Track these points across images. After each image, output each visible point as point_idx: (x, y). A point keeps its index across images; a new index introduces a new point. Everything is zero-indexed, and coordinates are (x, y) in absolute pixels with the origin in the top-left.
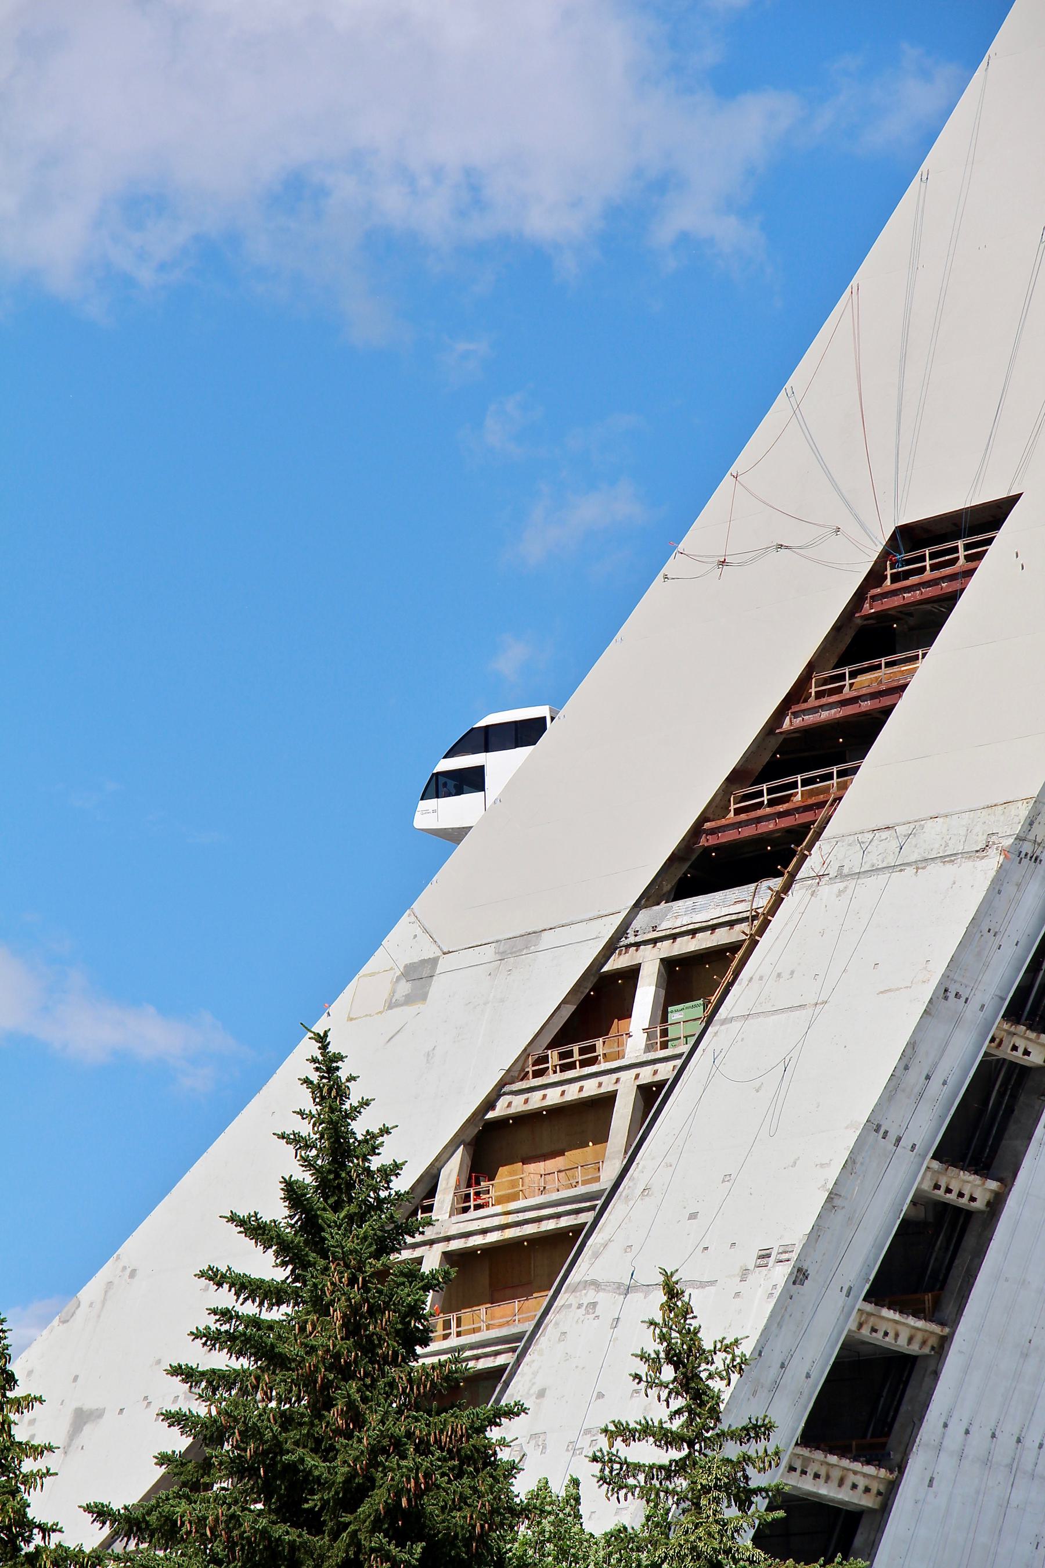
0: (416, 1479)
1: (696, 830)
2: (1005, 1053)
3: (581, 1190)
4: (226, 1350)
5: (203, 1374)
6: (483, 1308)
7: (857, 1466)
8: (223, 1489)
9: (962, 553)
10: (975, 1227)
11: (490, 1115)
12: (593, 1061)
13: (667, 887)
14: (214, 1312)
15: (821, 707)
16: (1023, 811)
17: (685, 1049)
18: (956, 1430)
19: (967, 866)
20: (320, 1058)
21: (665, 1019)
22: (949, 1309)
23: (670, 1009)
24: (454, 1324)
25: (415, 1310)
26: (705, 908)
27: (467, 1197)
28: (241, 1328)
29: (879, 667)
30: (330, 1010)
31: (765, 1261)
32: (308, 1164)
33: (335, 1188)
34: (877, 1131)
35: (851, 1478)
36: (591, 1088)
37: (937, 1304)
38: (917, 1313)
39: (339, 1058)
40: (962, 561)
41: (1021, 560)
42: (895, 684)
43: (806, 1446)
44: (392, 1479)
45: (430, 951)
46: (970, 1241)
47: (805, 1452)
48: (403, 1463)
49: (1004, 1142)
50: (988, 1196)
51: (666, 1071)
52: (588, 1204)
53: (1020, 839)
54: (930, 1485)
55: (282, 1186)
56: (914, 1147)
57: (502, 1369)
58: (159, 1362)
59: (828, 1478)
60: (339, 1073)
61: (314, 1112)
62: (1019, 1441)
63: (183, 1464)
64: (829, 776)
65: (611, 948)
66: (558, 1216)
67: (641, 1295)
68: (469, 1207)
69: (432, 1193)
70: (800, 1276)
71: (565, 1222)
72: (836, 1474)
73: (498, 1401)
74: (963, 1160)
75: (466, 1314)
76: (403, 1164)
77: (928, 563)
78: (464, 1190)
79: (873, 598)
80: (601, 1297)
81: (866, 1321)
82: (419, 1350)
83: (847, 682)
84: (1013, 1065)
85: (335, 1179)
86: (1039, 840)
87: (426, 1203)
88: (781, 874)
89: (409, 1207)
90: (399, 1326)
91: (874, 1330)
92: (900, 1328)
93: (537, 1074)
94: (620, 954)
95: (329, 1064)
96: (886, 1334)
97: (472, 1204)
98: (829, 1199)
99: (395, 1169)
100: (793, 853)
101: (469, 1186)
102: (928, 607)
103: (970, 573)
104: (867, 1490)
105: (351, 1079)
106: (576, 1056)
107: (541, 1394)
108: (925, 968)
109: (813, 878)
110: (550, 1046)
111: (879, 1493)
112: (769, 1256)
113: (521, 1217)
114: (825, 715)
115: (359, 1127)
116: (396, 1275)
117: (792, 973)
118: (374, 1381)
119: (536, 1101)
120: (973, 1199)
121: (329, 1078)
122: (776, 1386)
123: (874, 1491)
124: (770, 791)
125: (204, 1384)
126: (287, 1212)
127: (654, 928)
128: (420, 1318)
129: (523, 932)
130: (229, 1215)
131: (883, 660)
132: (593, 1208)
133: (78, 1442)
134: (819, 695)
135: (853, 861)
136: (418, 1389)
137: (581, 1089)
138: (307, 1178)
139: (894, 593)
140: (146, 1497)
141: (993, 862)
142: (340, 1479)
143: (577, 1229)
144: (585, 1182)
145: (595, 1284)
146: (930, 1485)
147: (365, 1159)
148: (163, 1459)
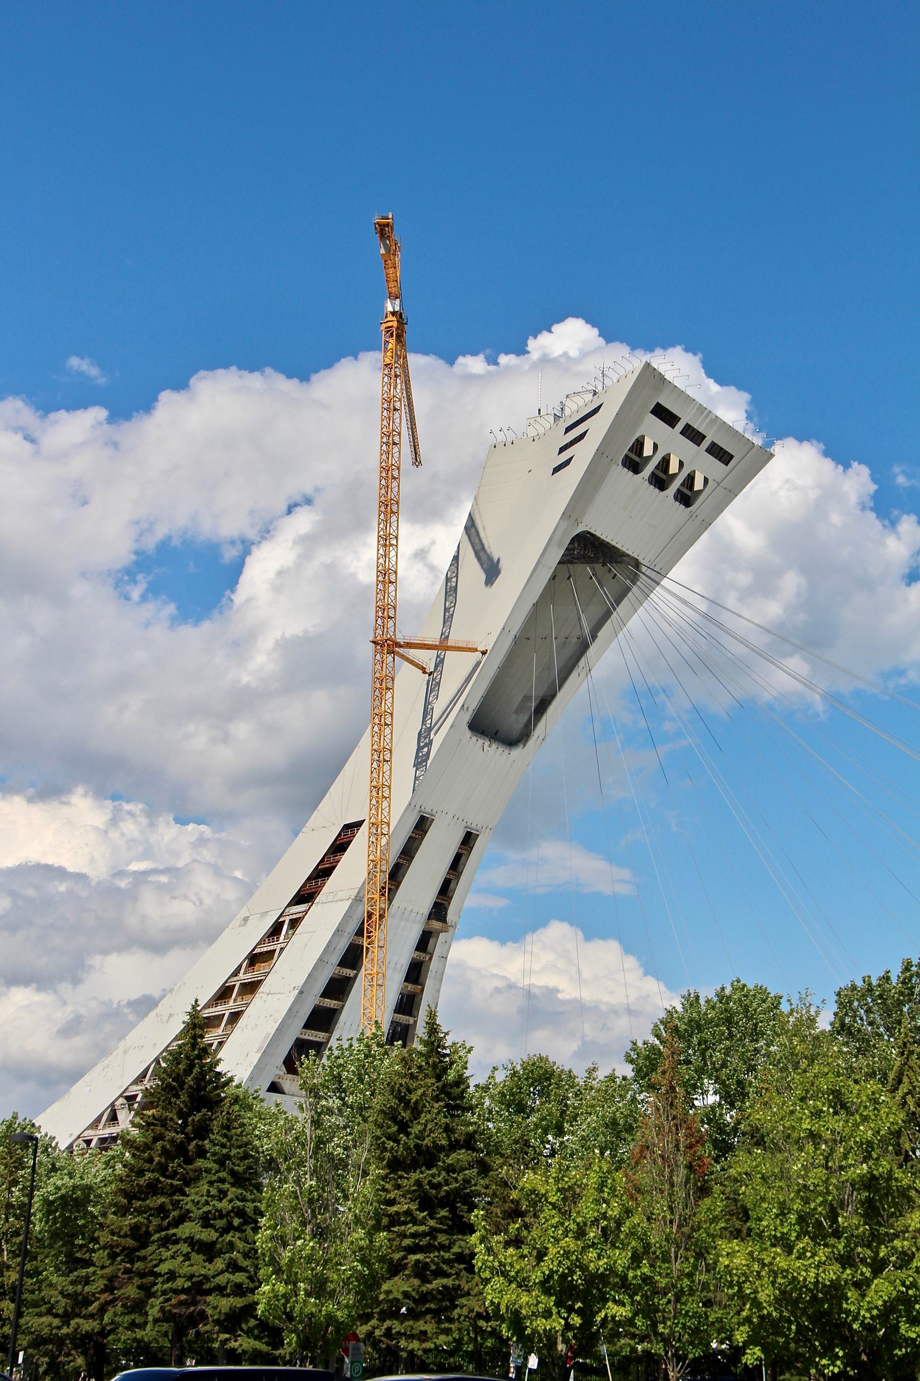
22: (345, 999)
37: (343, 997)
46: (350, 983)
65: (280, 916)
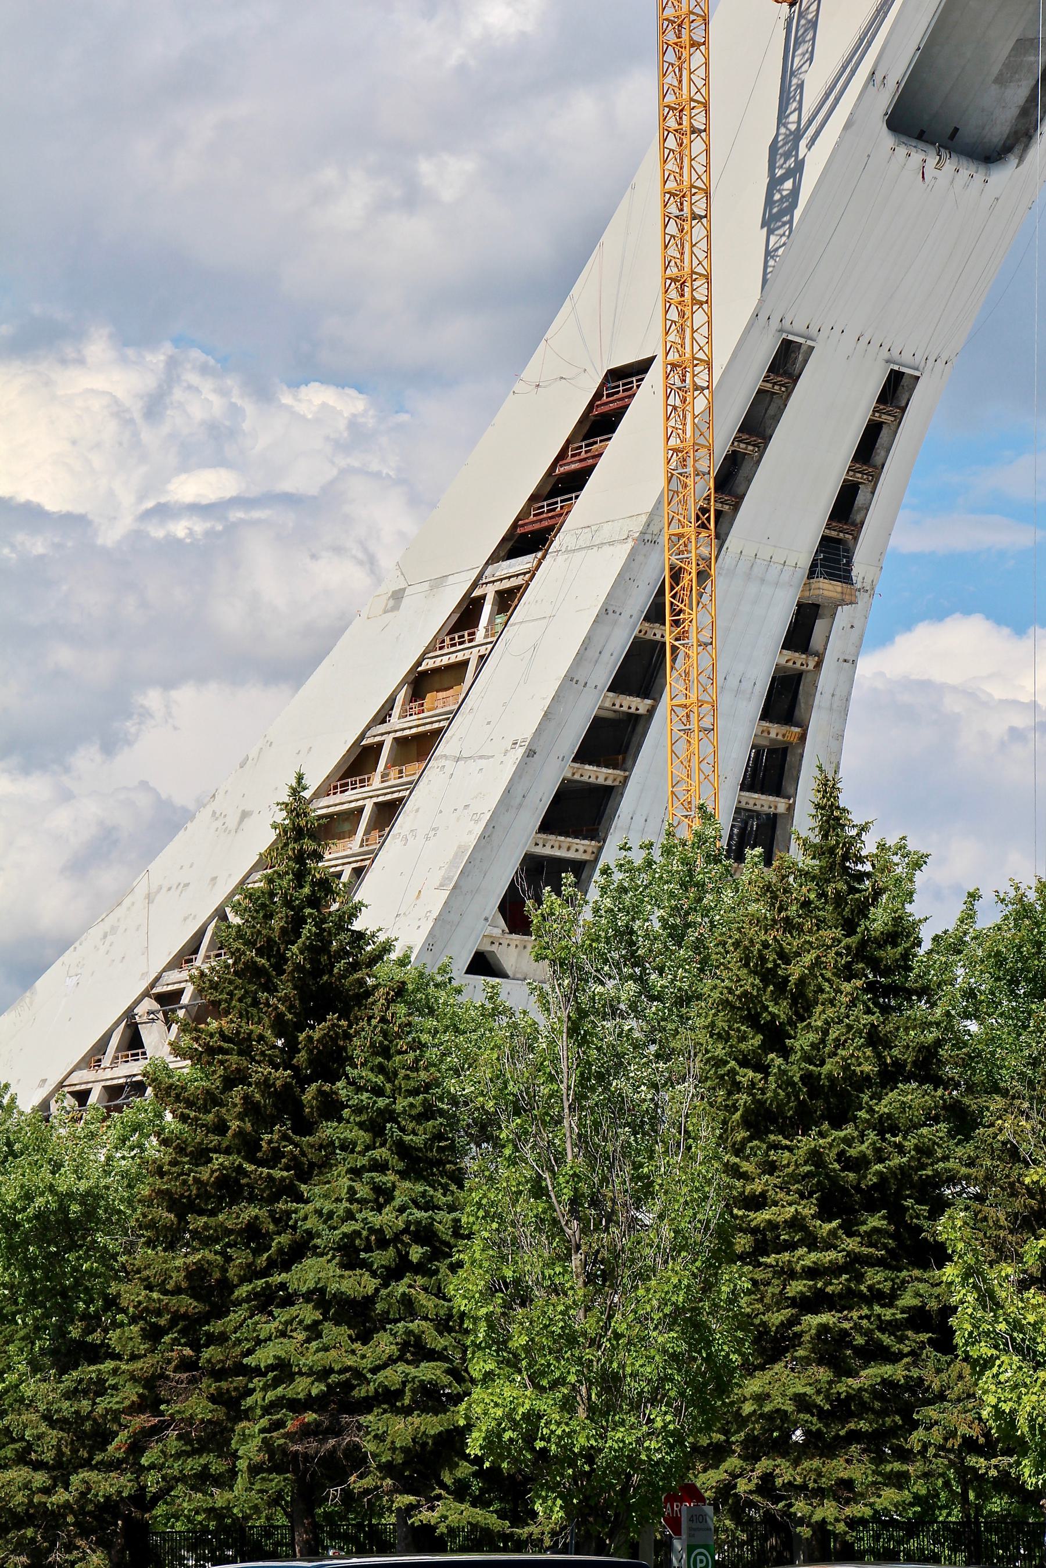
1: (515, 525)
11: (420, 669)
13: (502, 554)
16: (644, 519)
17: (495, 639)
26: (514, 566)
45: (403, 585)
65: (475, 585)
70: (531, 753)
79: (598, 406)
106: (457, 640)
114: (573, 466)
134: (573, 456)
141: (630, 544)
145: (445, 756)
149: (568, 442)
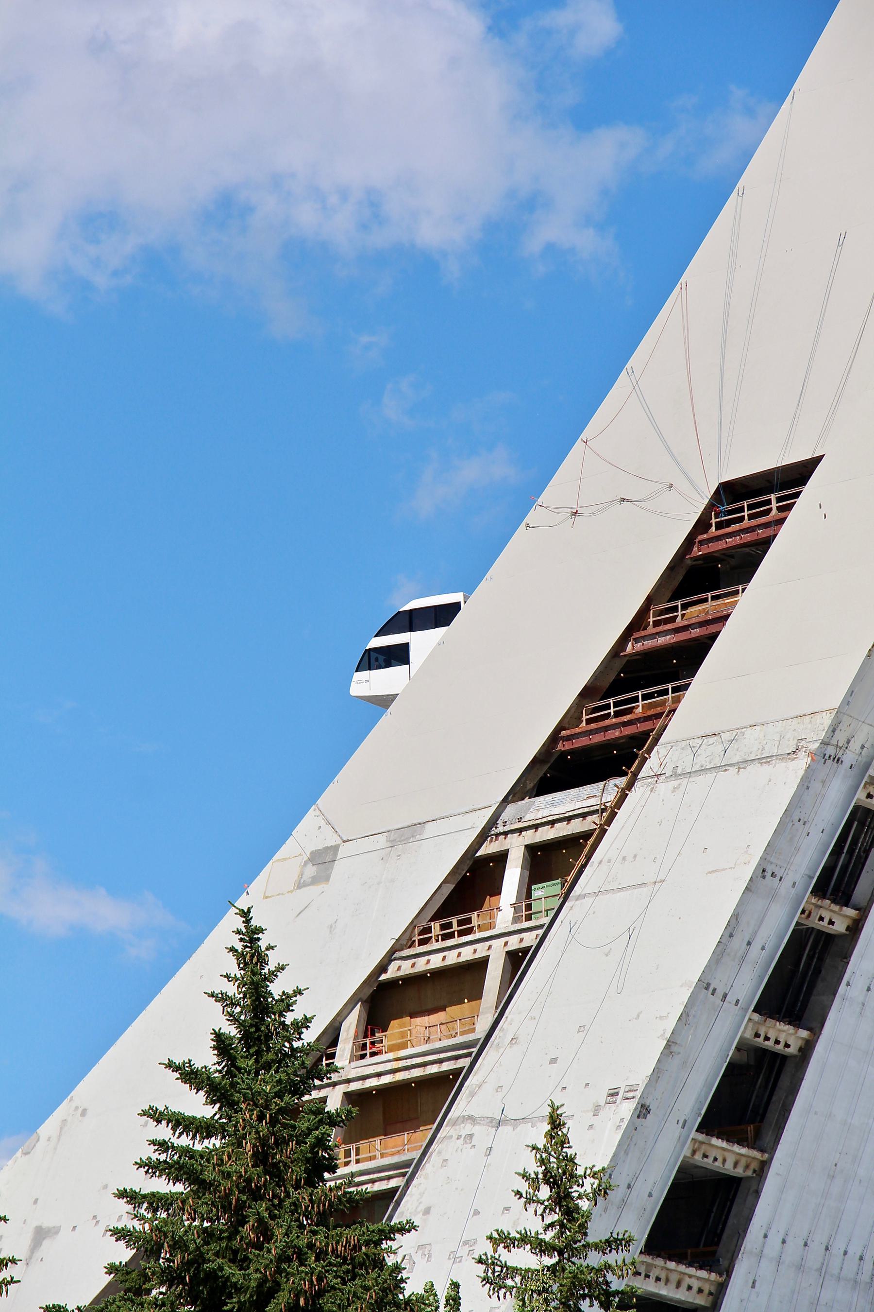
0: (311, 1282)
1: (554, 738)
2: (813, 923)
3: (460, 1039)
4: (164, 1177)
5: (144, 1197)
6: (377, 1140)
7: (692, 1271)
8: (161, 1293)
9: (774, 505)
10: (789, 1069)
11: (383, 977)
12: (470, 931)
13: (530, 785)
14: (153, 1143)
15: (658, 634)
16: (827, 720)
17: (546, 920)
18: (775, 1240)
19: (781, 766)
20: (244, 930)
21: (529, 895)
22: (768, 1138)
23: (533, 887)
24: (353, 1153)
25: (321, 1142)
26: (561, 802)
27: (364, 1047)
28: (176, 1158)
29: (706, 600)
30: (249, 890)
31: (614, 1098)
32: (233, 1019)
33: (256, 1039)
34: (707, 988)
35: (687, 1281)
36: (467, 954)
37: (758, 1134)
38: (741, 1141)
39: (260, 930)
40: (774, 511)
41: (824, 511)
42: (720, 614)
43: (649, 1254)
44: (293, 1283)
45: (332, 840)
46: (785, 1081)
47: (648, 1259)
48: (302, 1268)
49: (813, 998)
50: (800, 1043)
51: (530, 939)
52: (465, 1051)
53: (825, 743)
54: (753, 1286)
55: (213, 1037)
56: (737, 1002)
57: (394, 1190)
58: (106, 1187)
59: (667, 1281)
60: (260, 943)
61: (239, 976)
62: (827, 1249)
63: (128, 1273)
64: (665, 692)
65: (484, 836)
66: (440, 1061)
67: (510, 1128)
68: (366, 1054)
69: (334, 1043)
70: (643, 1111)
71: (446, 1067)
72: (674, 1277)
73: (390, 1218)
74: (779, 1013)
75: (363, 1145)
76: (312, 1018)
77: (746, 513)
78: (361, 1040)
79: (701, 543)
80: (477, 1130)
81: (699, 1149)
82: (326, 1175)
83: (680, 613)
84: (820, 933)
85: (255, 1032)
86: (840, 745)
87: (330, 1051)
88: (625, 774)
89: (316, 1054)
90: (309, 1155)
91: (705, 1156)
92: (727, 1154)
93: (423, 942)
94: (491, 841)
95: (251, 935)
96: (715, 1159)
97: (368, 1051)
98: (668, 1046)
99: (306, 1022)
100: (636, 756)
101: (365, 1036)
102: (747, 550)
103: (781, 522)
104: (700, 1291)
105: (270, 948)
106: (455, 927)
107: (427, 1211)
108: (746, 852)
109: (652, 777)
110: (433, 919)
111: (710, 1294)
112: (617, 1094)
113: (409, 1062)
114: (661, 641)
115: (276, 989)
116: (306, 1113)
117: (635, 856)
118: (281, 1201)
119: (421, 965)
120: (787, 1046)
121: (251, 947)
122: (624, 1203)
123: (706, 1292)
124: (616, 704)
125: (145, 1205)
126: (216, 1059)
127: (520, 820)
128: (327, 1148)
129: (409, 823)
130: (167, 1062)
131: (710, 595)
132: (469, 1055)
133: (38, 1254)
134: (656, 624)
135: (685, 763)
136: (318, 1207)
137: (459, 955)
138: (231, 1030)
139: (718, 538)
140: (96, 1300)
141: (802, 763)
142: (253, 1284)
143: (457, 1072)
144: (463, 1033)
145: (472, 1119)
146: (753, 1286)
147: (281, 1015)
148: (112, 1269)
149: (649, 601)
